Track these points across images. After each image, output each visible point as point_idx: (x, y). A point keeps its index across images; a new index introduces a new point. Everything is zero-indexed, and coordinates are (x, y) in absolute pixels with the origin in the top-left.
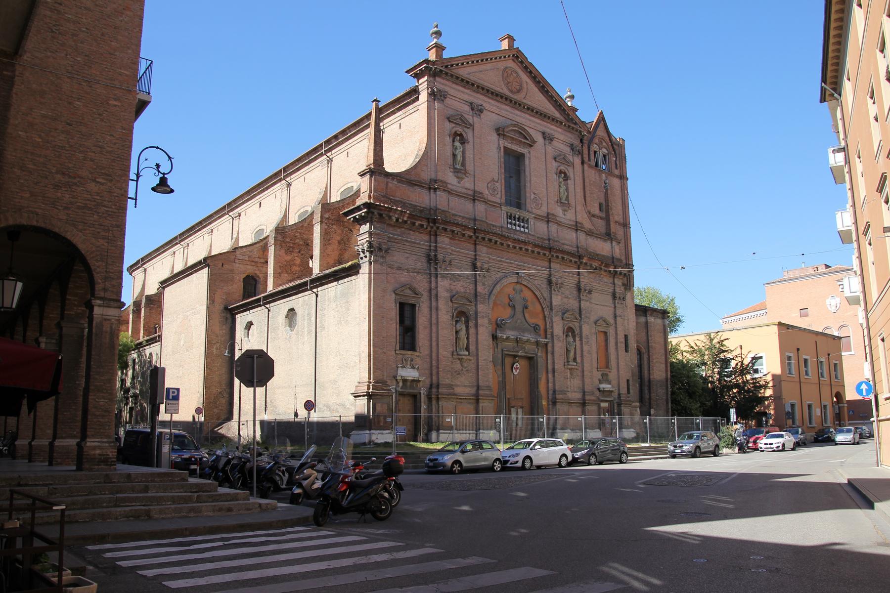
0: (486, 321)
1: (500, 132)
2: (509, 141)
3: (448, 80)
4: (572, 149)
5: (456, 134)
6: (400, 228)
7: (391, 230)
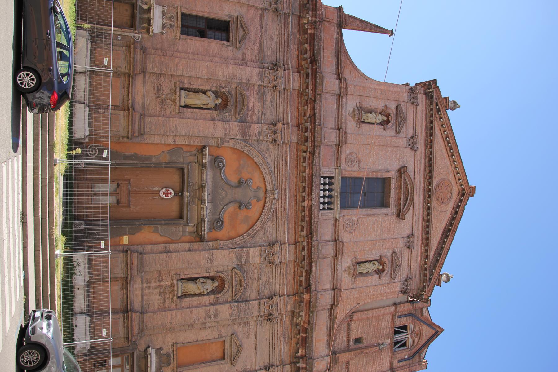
0: (220, 134)
1: (401, 171)
2: (397, 184)
3: (426, 108)
4: (406, 280)
5: (388, 116)
6: (299, 31)
7: (295, 21)
